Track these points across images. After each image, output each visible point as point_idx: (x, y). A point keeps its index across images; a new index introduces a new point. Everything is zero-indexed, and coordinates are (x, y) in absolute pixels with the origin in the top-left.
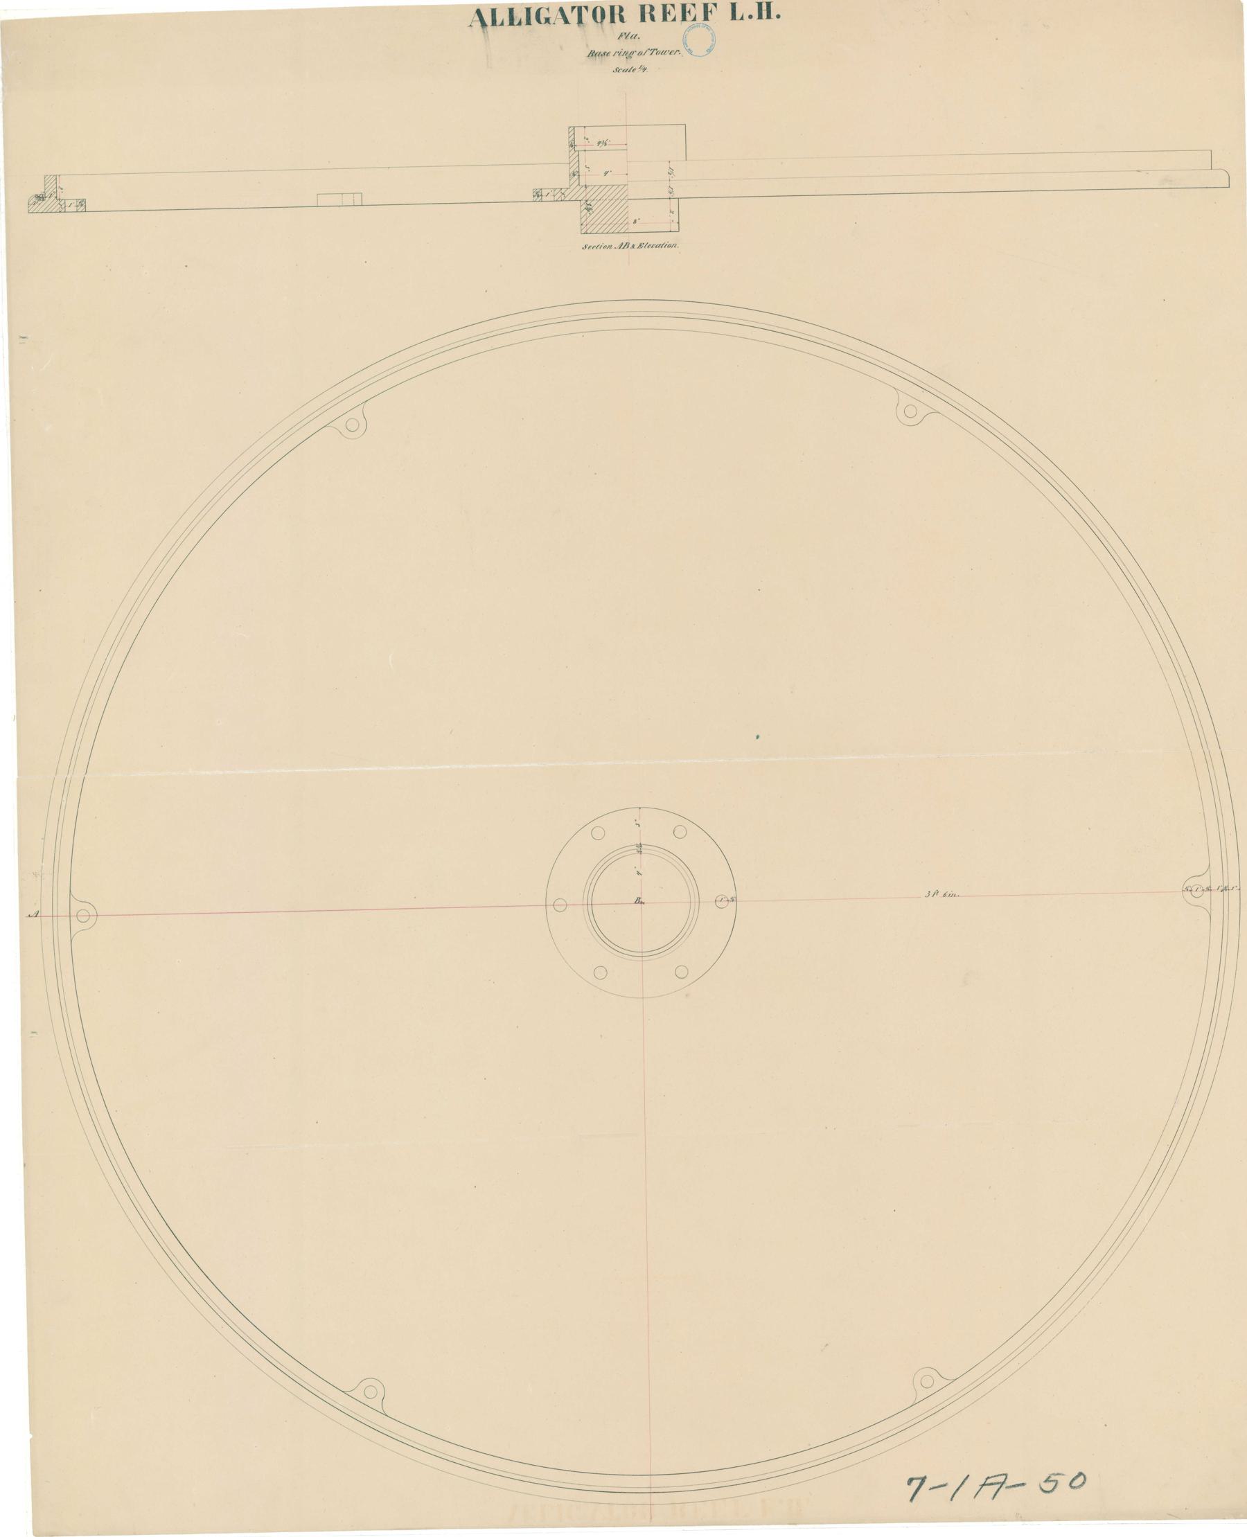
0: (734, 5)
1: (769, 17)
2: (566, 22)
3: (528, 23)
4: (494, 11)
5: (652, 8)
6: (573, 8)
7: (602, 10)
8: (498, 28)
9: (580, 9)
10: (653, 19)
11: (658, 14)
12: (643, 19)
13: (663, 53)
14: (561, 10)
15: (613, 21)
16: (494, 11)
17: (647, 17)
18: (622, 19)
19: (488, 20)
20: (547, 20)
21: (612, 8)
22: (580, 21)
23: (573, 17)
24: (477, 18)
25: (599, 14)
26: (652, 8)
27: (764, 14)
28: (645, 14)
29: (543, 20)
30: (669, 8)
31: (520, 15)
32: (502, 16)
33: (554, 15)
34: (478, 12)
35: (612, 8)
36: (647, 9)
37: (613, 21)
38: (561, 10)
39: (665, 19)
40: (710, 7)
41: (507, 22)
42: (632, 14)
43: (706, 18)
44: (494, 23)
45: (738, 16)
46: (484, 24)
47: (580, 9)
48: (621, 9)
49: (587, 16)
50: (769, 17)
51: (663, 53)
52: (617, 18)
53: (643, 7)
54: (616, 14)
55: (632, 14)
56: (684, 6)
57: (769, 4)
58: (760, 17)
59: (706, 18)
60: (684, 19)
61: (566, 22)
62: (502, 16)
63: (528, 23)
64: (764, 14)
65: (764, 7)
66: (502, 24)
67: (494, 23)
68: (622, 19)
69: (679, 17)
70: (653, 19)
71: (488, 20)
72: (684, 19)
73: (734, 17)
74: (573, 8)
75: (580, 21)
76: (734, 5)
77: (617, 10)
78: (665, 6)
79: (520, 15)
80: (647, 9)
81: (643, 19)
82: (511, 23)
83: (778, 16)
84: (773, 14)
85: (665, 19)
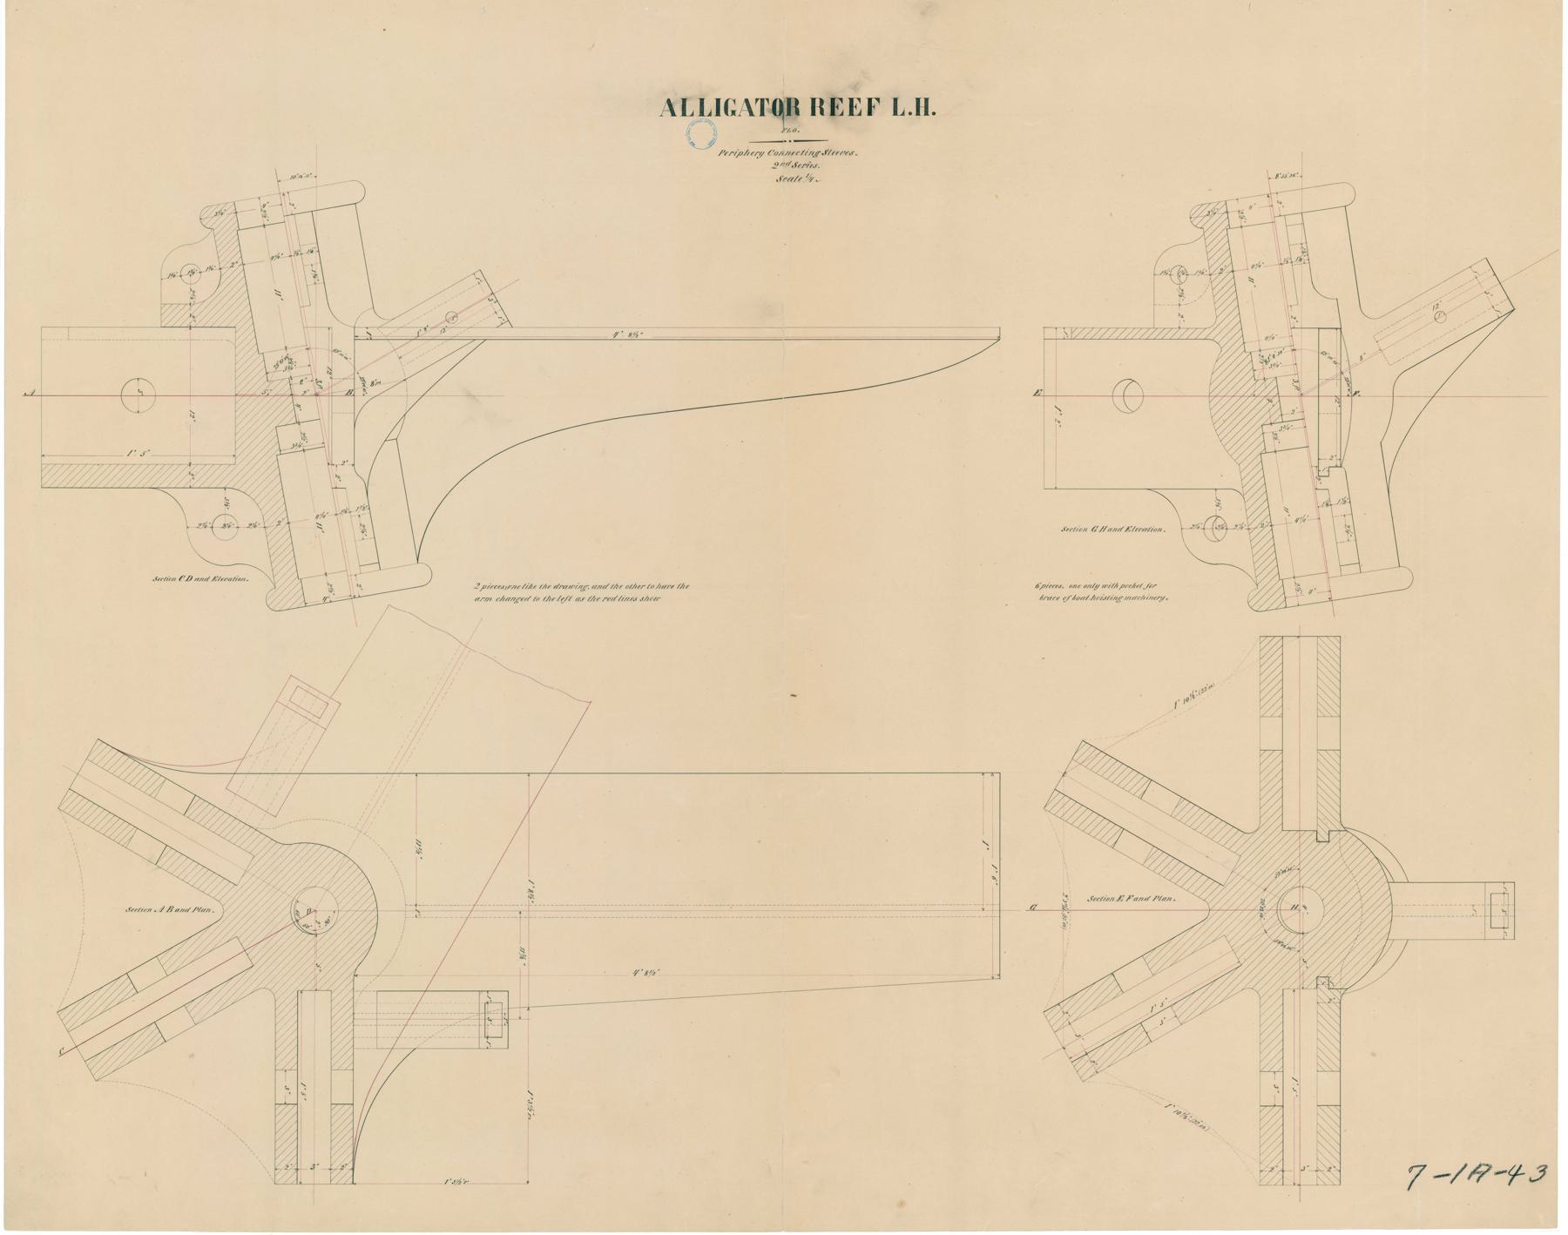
2: (751, 114)
3: (718, 114)
8: (688, 119)
16: (684, 101)
19: (678, 109)
22: (762, 114)
23: (756, 108)
27: (922, 111)
31: (710, 106)
32: (693, 106)
33: (740, 107)
39: (833, 113)
40: (874, 102)
41: (697, 112)
43: (870, 113)
48: (797, 102)
59: (870, 113)
60: (851, 113)
61: (751, 114)
62: (693, 106)
63: (718, 114)
64: (922, 111)
71: (678, 109)
72: (851, 113)
73: (895, 113)
75: (762, 114)
78: (833, 100)
79: (710, 106)
81: (813, 114)
82: (702, 114)
85: (833, 113)
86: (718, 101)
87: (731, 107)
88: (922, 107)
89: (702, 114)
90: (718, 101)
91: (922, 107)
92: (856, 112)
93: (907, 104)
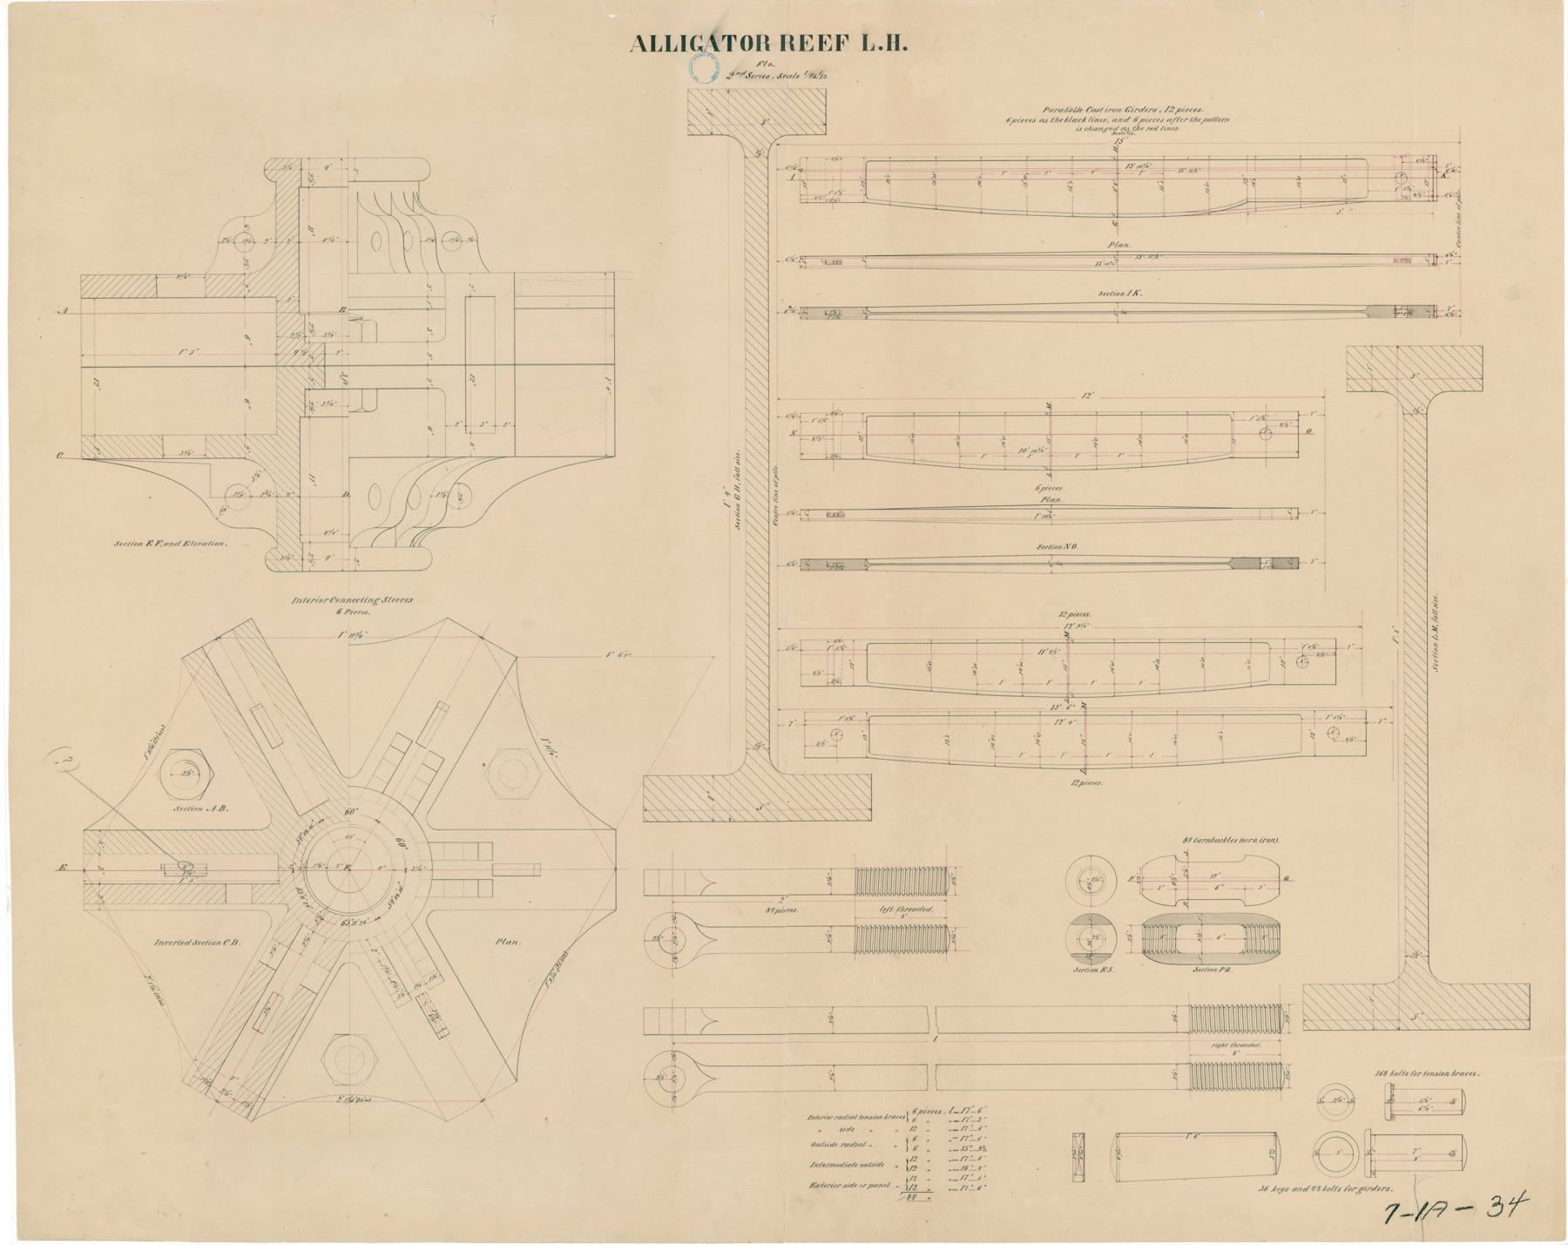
0: (865, 37)
2: (716, 49)
3: (684, 49)
4: (653, 38)
8: (656, 54)
11: (797, 43)
12: (783, 49)
14: (712, 38)
16: (653, 38)
17: (787, 46)
19: (648, 46)
21: (759, 37)
22: (729, 49)
23: (723, 45)
25: (749, 43)
27: (893, 46)
31: (676, 42)
32: (660, 42)
35: (759, 37)
36: (787, 39)
39: (802, 49)
40: (843, 38)
42: (775, 42)
44: (653, 49)
49: (736, 44)
52: (763, 46)
53: (783, 37)
61: (716, 49)
62: (660, 42)
63: (684, 49)
64: (893, 46)
67: (653, 49)
75: (729, 49)
76: (865, 37)
77: (763, 39)
78: (802, 37)
79: (676, 42)
81: (783, 49)
82: (668, 49)
85: (802, 49)
87: (697, 43)
88: (893, 42)
89: (668, 49)
91: (893, 42)
93: (878, 39)
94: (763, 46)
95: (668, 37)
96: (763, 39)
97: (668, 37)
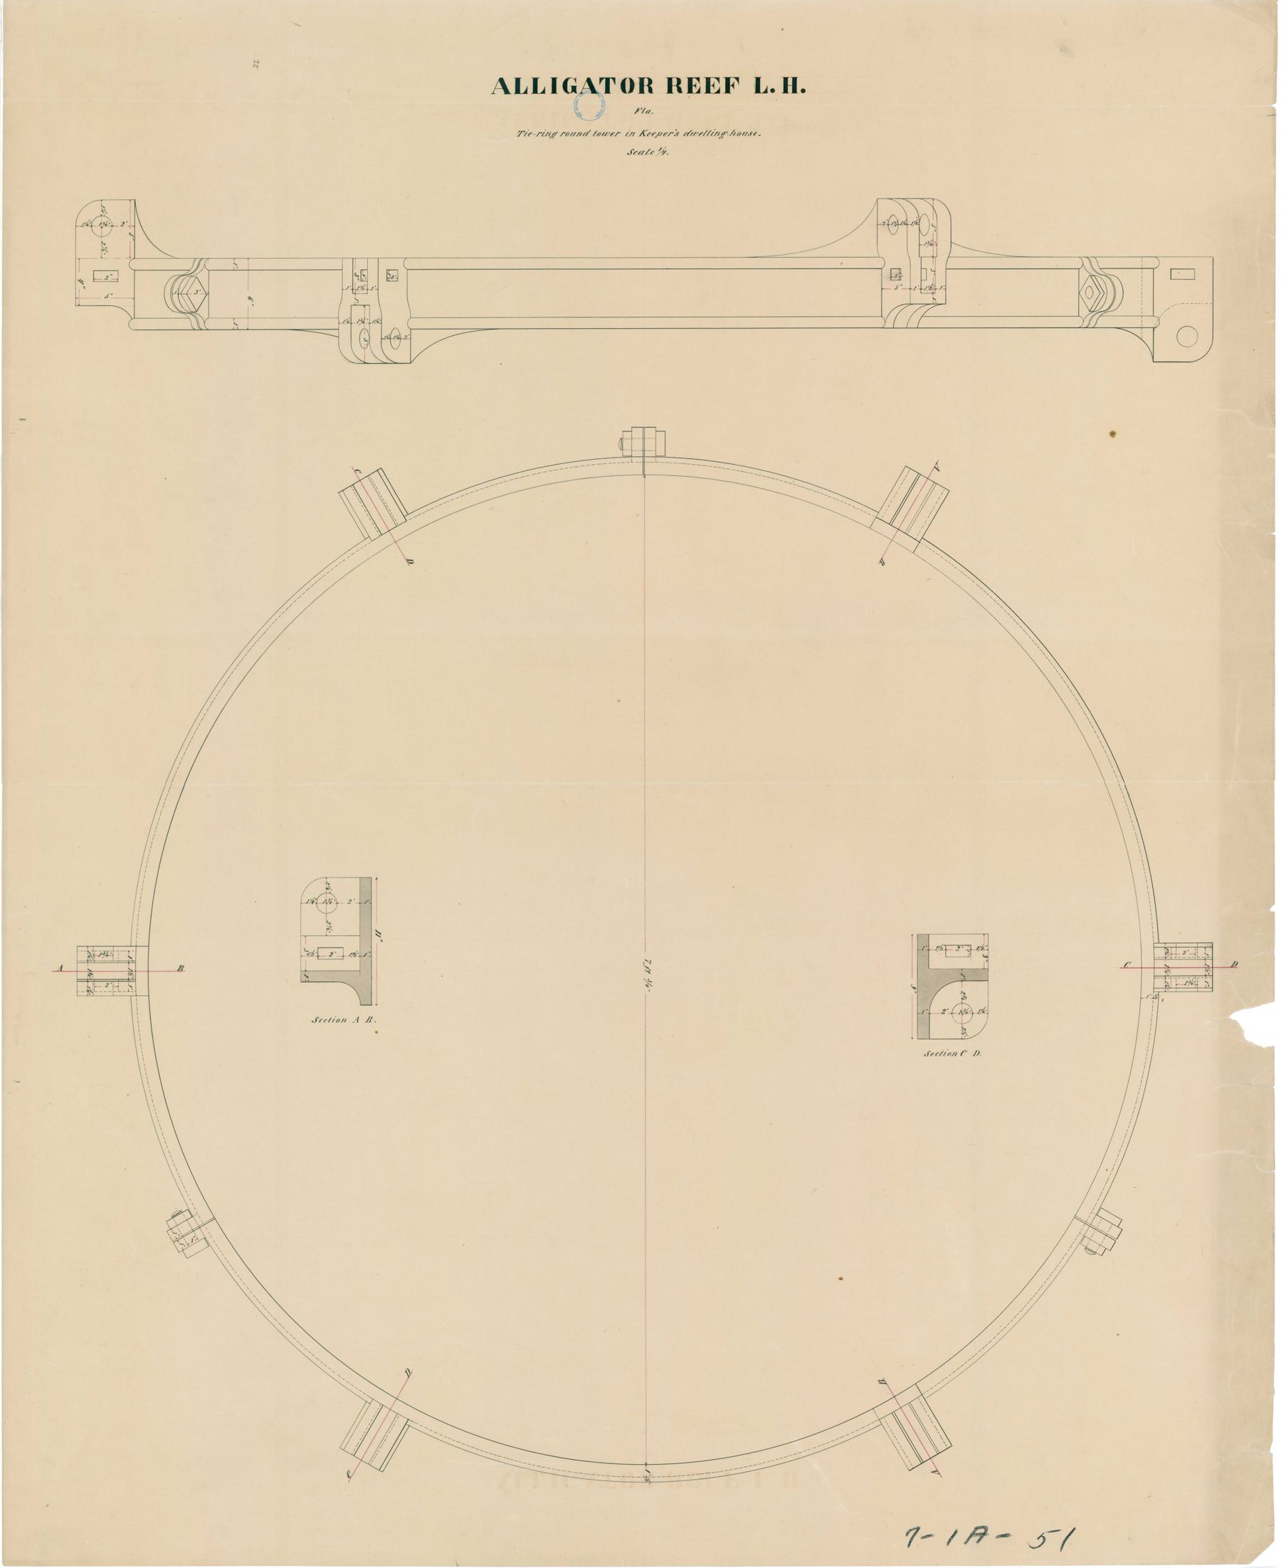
0: (758, 80)
1: (794, 91)
3: (554, 91)
4: (518, 80)
5: (679, 81)
6: (601, 79)
7: (631, 81)
9: (608, 80)
10: (680, 90)
11: (684, 86)
12: (670, 91)
13: (605, 134)
14: (589, 81)
15: (642, 91)
16: (518, 80)
17: (675, 89)
18: (650, 91)
19: (512, 88)
20: (574, 89)
22: (607, 91)
23: (600, 88)
24: (499, 86)
25: (627, 86)
26: (679, 81)
27: (790, 89)
28: (672, 85)
29: (569, 89)
30: (695, 81)
31: (545, 83)
32: (526, 84)
33: (581, 85)
34: (501, 81)
35: (642, 80)
36: (675, 82)
37: (642, 91)
38: (589, 81)
40: (732, 81)
41: (531, 90)
42: (660, 85)
43: (728, 91)
45: (762, 90)
46: (507, 92)
47: (608, 80)
48: (650, 81)
49: (615, 88)
50: (794, 91)
51: (605, 134)
52: (646, 89)
53: (670, 80)
54: (645, 85)
55: (660, 85)
56: (708, 80)
57: (795, 80)
58: (786, 91)
59: (728, 91)
60: (708, 91)
62: (526, 84)
63: (554, 91)
64: (790, 89)
65: (790, 82)
66: (544, 92)
67: (518, 91)
68: (650, 91)
69: (703, 90)
70: (680, 90)
71: (512, 88)
72: (708, 91)
73: (758, 91)
74: (601, 79)
75: (607, 91)
76: (758, 80)
77: (646, 82)
78: (690, 80)
79: (545, 83)
80: (675, 82)
81: (670, 91)
82: (535, 91)
83: (803, 91)
84: (799, 89)
85: (690, 91)
86: (554, 80)
87: (570, 84)
89: (535, 91)
90: (554, 80)
91: (790, 85)
92: (695, 90)
94: (646, 89)
95: (535, 80)
96: (646, 82)
97: (535, 80)
